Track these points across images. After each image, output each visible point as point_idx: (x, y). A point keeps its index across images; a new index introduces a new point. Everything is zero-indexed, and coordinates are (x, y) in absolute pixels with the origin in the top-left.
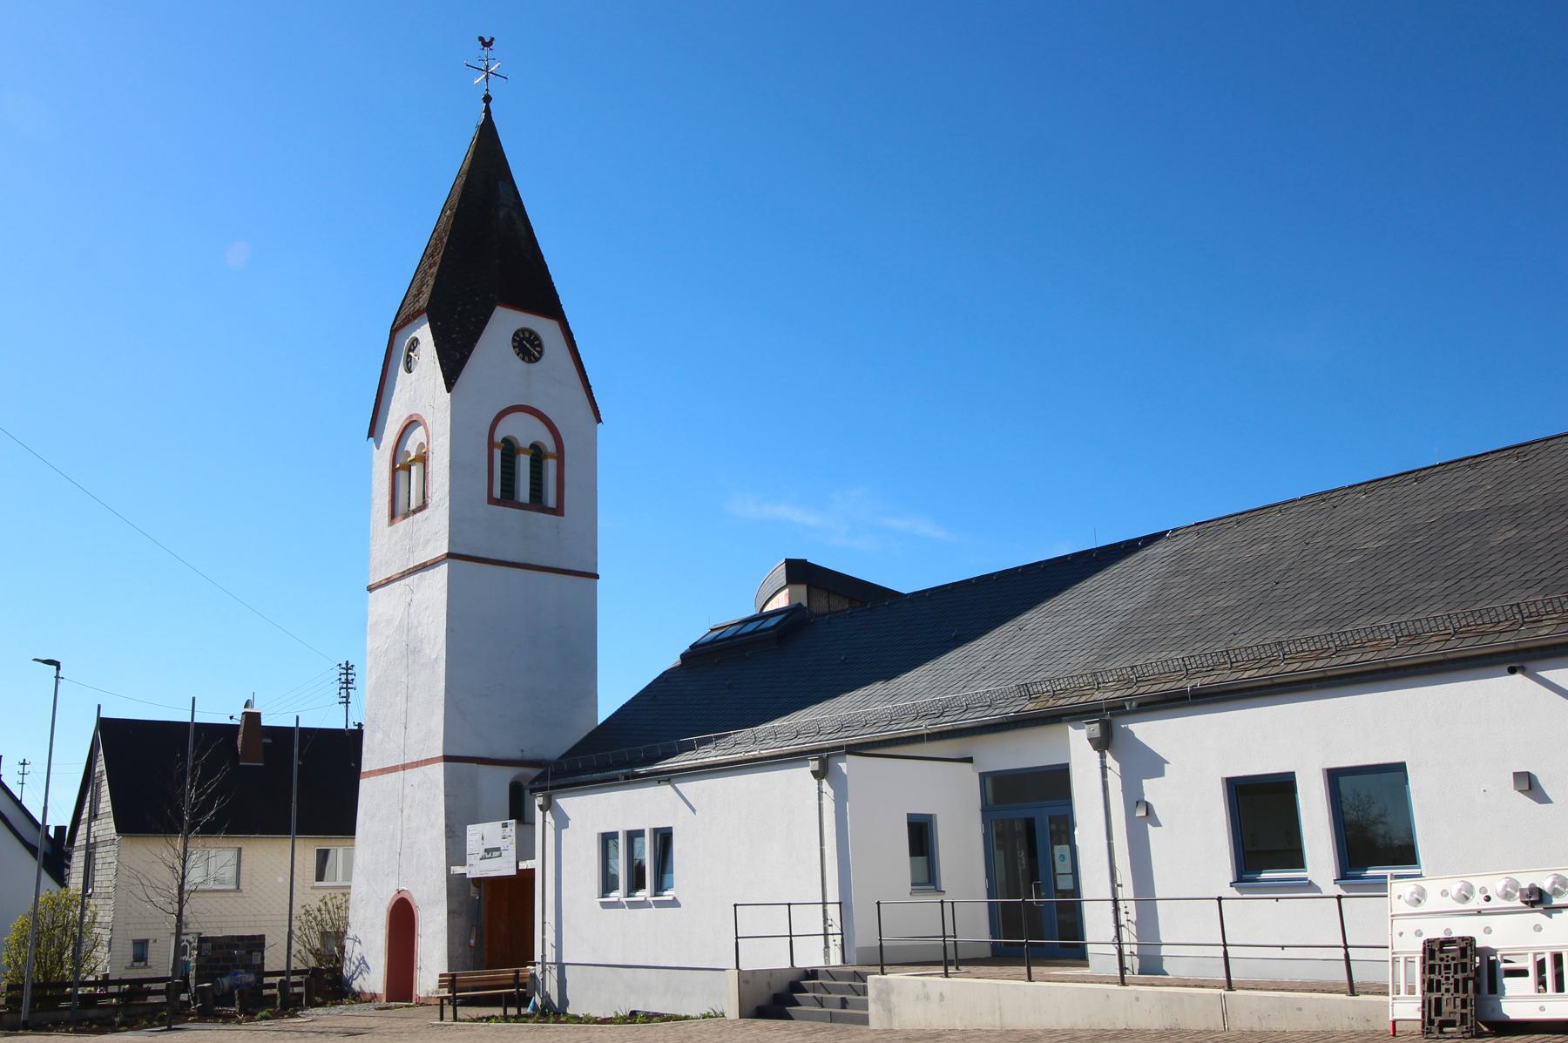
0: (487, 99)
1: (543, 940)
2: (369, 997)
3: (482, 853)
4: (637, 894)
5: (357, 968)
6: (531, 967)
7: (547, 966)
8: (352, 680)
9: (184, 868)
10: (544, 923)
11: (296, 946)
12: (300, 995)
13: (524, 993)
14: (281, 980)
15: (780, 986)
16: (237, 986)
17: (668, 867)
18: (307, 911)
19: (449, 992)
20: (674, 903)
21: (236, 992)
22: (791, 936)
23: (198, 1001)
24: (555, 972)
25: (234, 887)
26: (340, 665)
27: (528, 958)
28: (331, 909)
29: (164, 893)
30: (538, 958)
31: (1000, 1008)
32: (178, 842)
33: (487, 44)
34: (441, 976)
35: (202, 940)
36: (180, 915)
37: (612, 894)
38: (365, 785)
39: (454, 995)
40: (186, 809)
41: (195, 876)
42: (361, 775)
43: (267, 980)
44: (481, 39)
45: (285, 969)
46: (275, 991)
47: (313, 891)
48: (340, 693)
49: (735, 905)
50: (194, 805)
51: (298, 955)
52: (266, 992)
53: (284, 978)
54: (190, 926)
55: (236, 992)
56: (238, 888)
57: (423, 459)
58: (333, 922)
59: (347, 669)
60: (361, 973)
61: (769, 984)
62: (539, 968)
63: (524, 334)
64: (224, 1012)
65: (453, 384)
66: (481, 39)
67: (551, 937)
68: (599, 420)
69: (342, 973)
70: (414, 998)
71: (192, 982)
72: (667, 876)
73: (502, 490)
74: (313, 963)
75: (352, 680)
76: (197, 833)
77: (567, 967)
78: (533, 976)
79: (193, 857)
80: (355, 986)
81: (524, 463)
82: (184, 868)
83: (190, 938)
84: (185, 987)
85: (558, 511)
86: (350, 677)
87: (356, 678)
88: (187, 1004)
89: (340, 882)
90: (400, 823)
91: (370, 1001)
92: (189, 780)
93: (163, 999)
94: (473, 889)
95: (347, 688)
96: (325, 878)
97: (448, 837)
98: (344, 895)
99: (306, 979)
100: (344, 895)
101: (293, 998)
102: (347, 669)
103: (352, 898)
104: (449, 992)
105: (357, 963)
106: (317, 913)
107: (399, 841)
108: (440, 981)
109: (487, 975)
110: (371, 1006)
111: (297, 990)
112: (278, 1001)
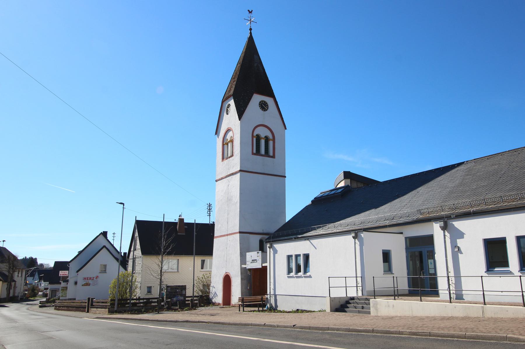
0: (251, 29)
1: (270, 288)
2: (217, 304)
3: (251, 261)
4: (299, 274)
5: (214, 295)
6: (266, 296)
7: (271, 295)
8: (211, 209)
9: (162, 265)
10: (270, 282)
11: (195, 289)
12: (197, 303)
13: (265, 303)
14: (191, 299)
15: (343, 302)
16: (178, 300)
17: (308, 266)
18: (199, 278)
19: (242, 303)
20: (310, 277)
21: (178, 302)
22: (346, 287)
23: (167, 304)
24: (273, 297)
25: (176, 271)
27: (265, 293)
28: (206, 277)
29: (156, 272)
30: (268, 293)
31: (412, 310)
32: (160, 257)
33: (250, 12)
34: (239, 298)
35: (167, 287)
36: (161, 279)
37: (291, 274)
38: (215, 240)
39: (243, 304)
40: (162, 248)
41: (165, 268)
42: (214, 237)
43: (187, 299)
44: (249, 11)
45: (192, 295)
46: (189, 302)
47: (200, 272)
49: (329, 277)
50: (165, 246)
51: (196, 291)
52: (187, 302)
53: (192, 298)
54: (164, 282)
55: (178, 302)
56: (178, 271)
57: (232, 141)
58: (206, 282)
59: (210, 205)
60: (215, 297)
61: (339, 302)
62: (269, 296)
64: (174, 308)
65: (241, 118)
66: (249, 11)
67: (272, 287)
68: (286, 129)
69: (209, 297)
70: (231, 305)
71: (165, 299)
72: (308, 268)
74: (200, 294)
75: (211, 209)
76: (165, 255)
77: (277, 296)
78: (267, 298)
79: (165, 262)
80: (213, 301)
81: (263, 142)
82: (162, 265)
83: (164, 286)
84: (163, 301)
85: (273, 157)
88: (163, 306)
89: (208, 270)
90: (226, 252)
91: (218, 305)
92: (163, 239)
93: (156, 304)
94: (248, 272)
95: (210, 211)
96: (204, 268)
97: (241, 256)
98: (210, 273)
99: (199, 299)
100: (210, 273)
101: (195, 304)
102: (210, 205)
103: (212, 274)
104: (242, 303)
105: (214, 294)
106: (202, 279)
107: (226, 257)
108: (239, 300)
109: (253, 298)
110: (218, 307)
111: (196, 302)
112: (191, 305)
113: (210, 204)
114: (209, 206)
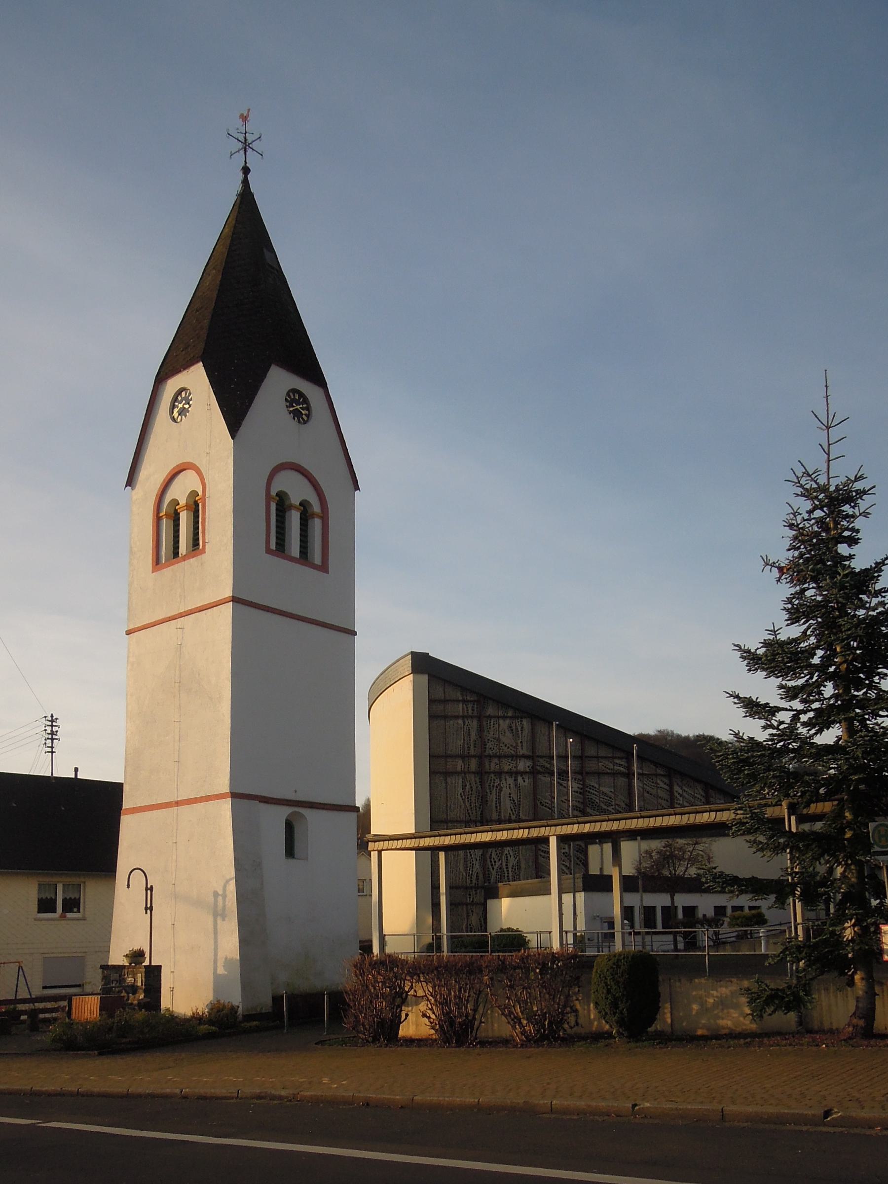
0: (246, 170)
8: (57, 731)
26: (45, 717)
48: (45, 743)
57: (195, 507)
59: (52, 721)
63: (289, 396)
65: (235, 436)
68: (357, 488)
73: (277, 543)
75: (57, 731)
81: (294, 518)
85: (324, 568)
86: (55, 729)
87: (59, 730)
95: (52, 739)
102: (52, 721)
113: (52, 716)
114: (50, 723)
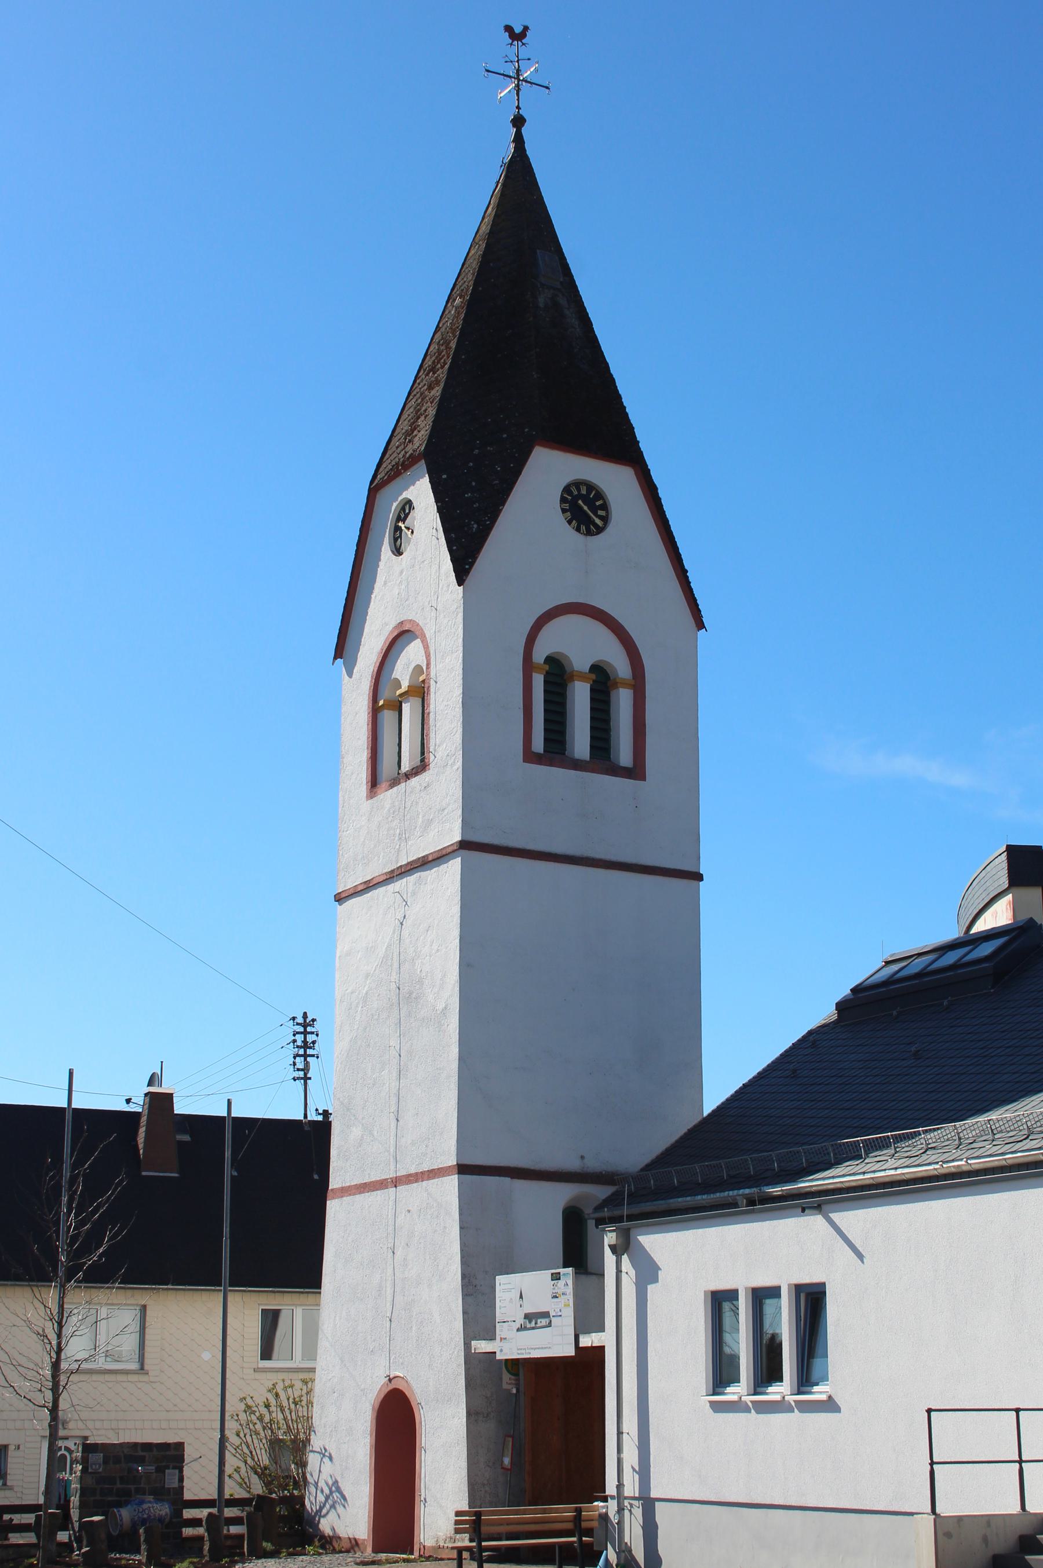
8: (314, 1042)
26: (294, 1019)
48: (294, 1064)
65: (467, 572)
75: (314, 1042)
81: (580, 696)
85: (636, 772)
86: (310, 1038)
87: (319, 1039)
95: (305, 1056)
102: (305, 1025)
